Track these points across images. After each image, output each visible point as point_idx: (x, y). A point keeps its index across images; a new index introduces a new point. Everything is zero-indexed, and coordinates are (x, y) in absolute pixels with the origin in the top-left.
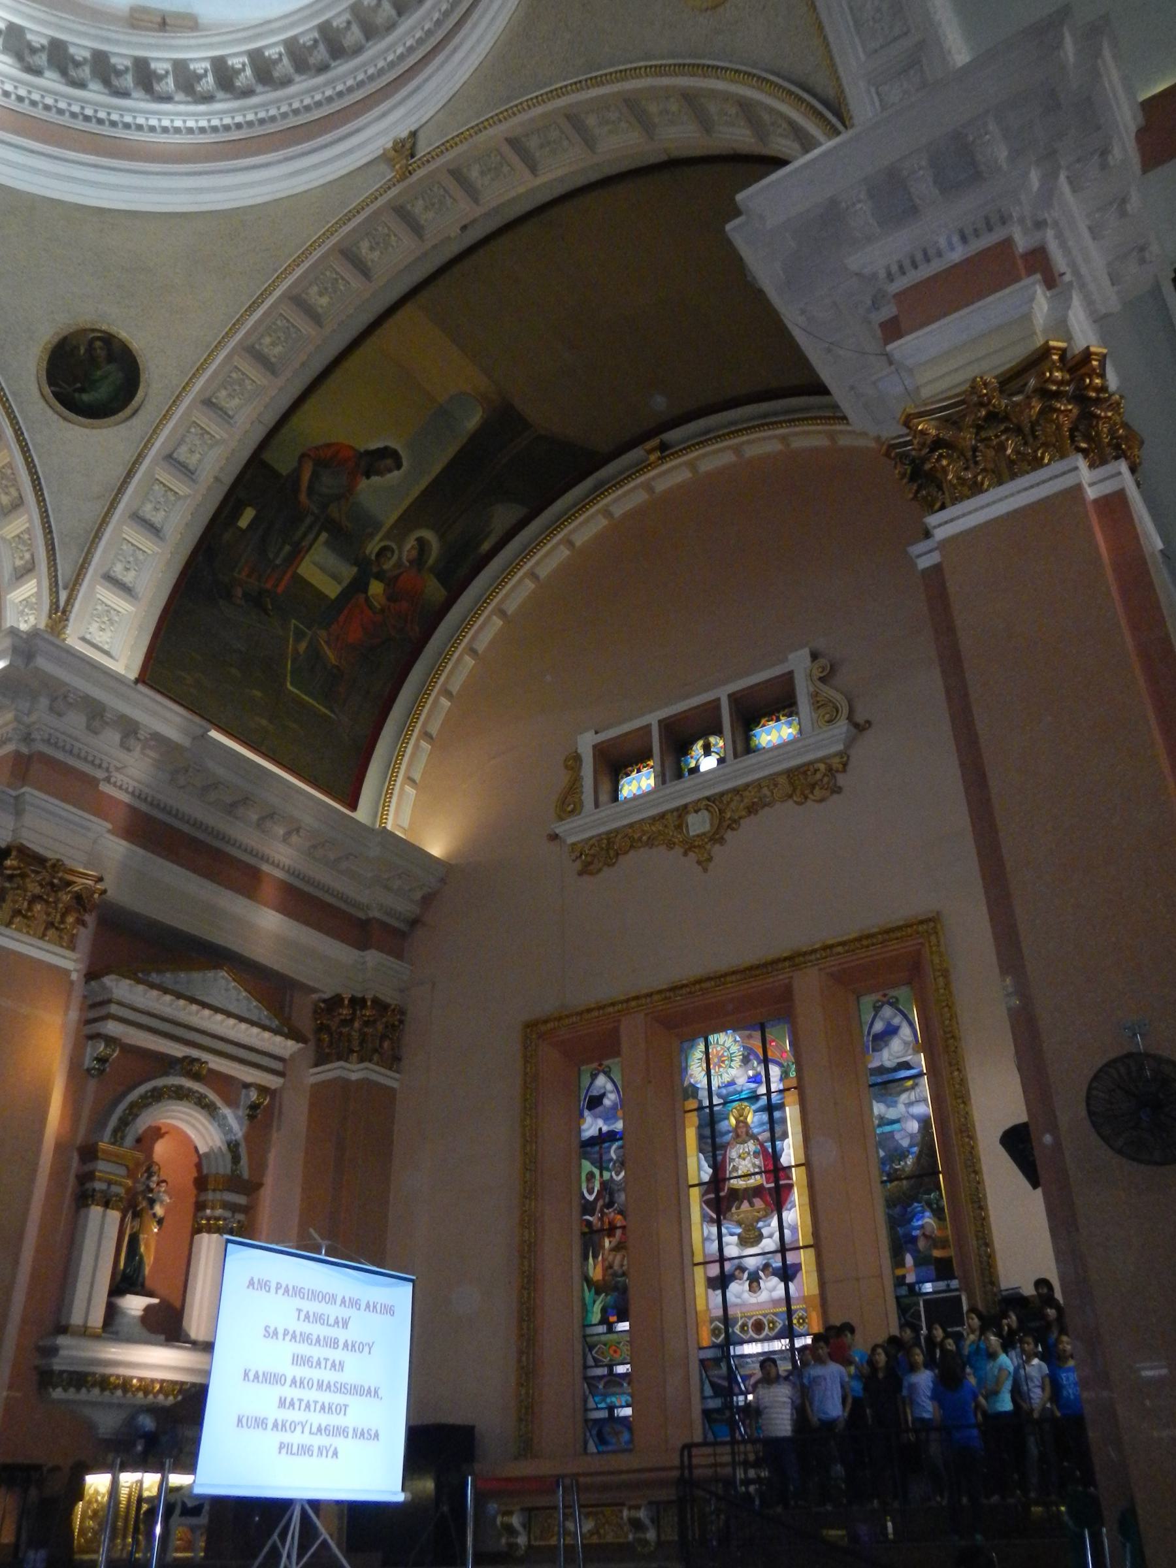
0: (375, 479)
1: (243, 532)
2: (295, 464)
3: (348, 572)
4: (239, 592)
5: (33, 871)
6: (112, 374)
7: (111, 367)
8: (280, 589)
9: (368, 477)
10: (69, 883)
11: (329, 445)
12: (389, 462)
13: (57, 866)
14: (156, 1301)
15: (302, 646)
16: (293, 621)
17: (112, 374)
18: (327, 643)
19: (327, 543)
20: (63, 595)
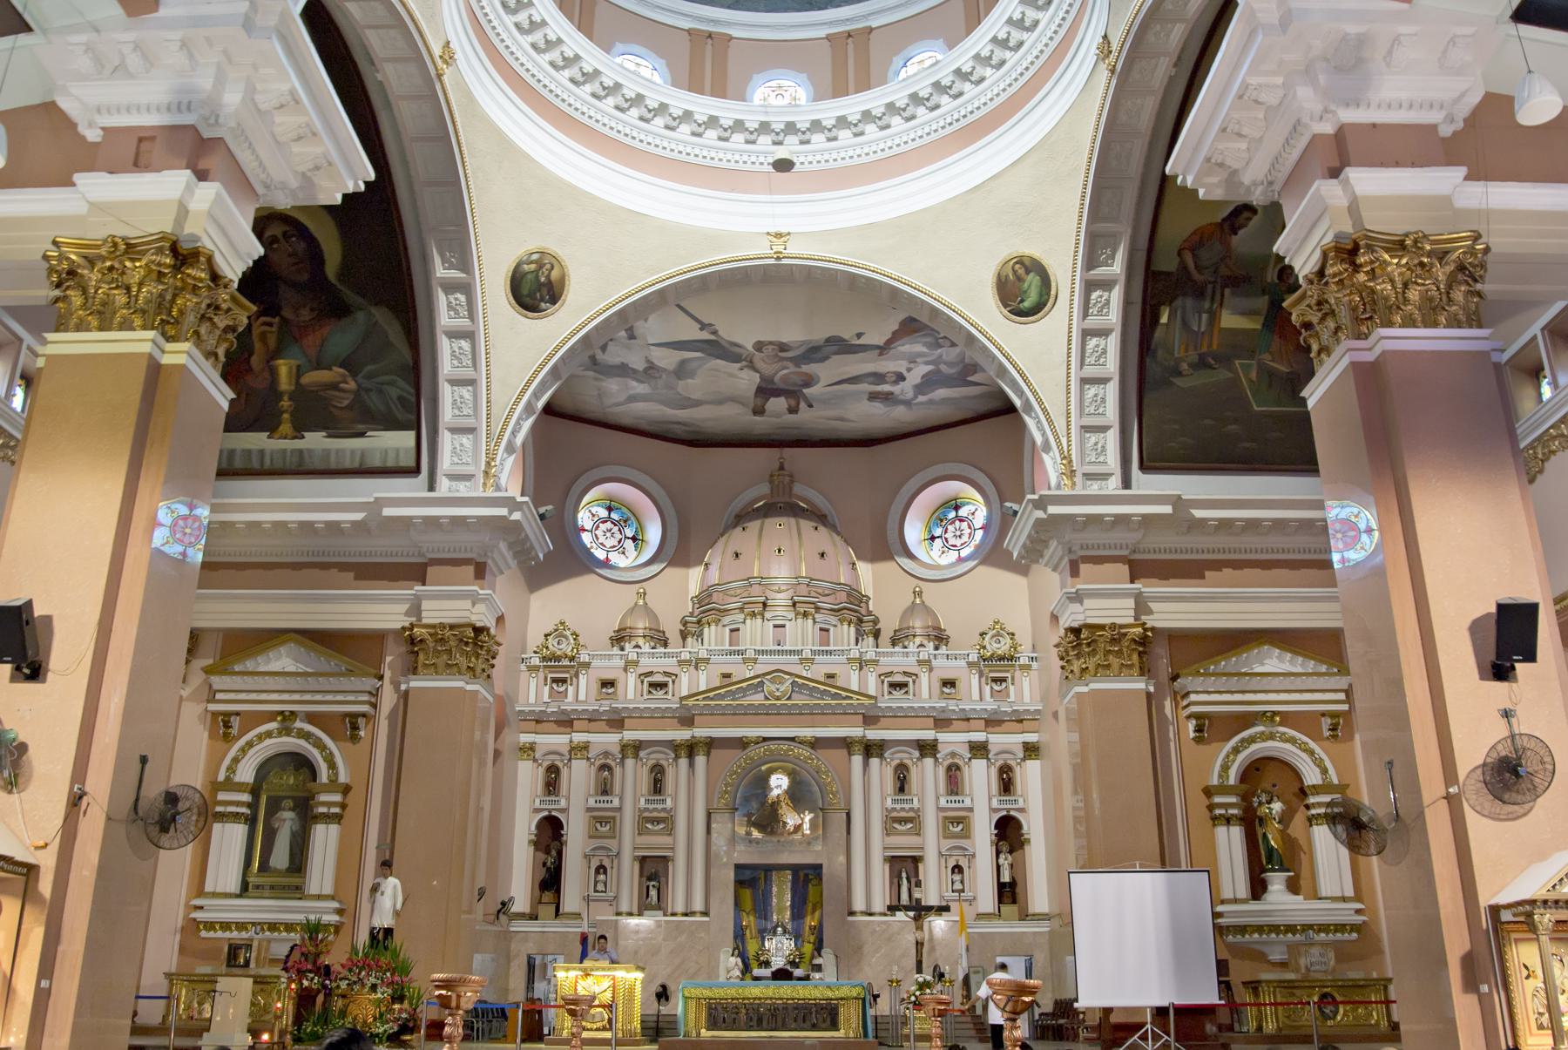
0: (1241, 232)
1: (1167, 324)
2: (1177, 260)
3: (1263, 302)
4: (1185, 366)
5: (1100, 636)
6: (1033, 280)
7: (1032, 275)
8: (1215, 347)
9: (1236, 234)
10: (1125, 634)
11: (1194, 233)
12: (1246, 214)
13: (1113, 626)
14: (1292, 874)
15: (1253, 375)
16: (1237, 362)
17: (1033, 280)
18: (1273, 361)
19: (1233, 294)
20: (1064, 441)
